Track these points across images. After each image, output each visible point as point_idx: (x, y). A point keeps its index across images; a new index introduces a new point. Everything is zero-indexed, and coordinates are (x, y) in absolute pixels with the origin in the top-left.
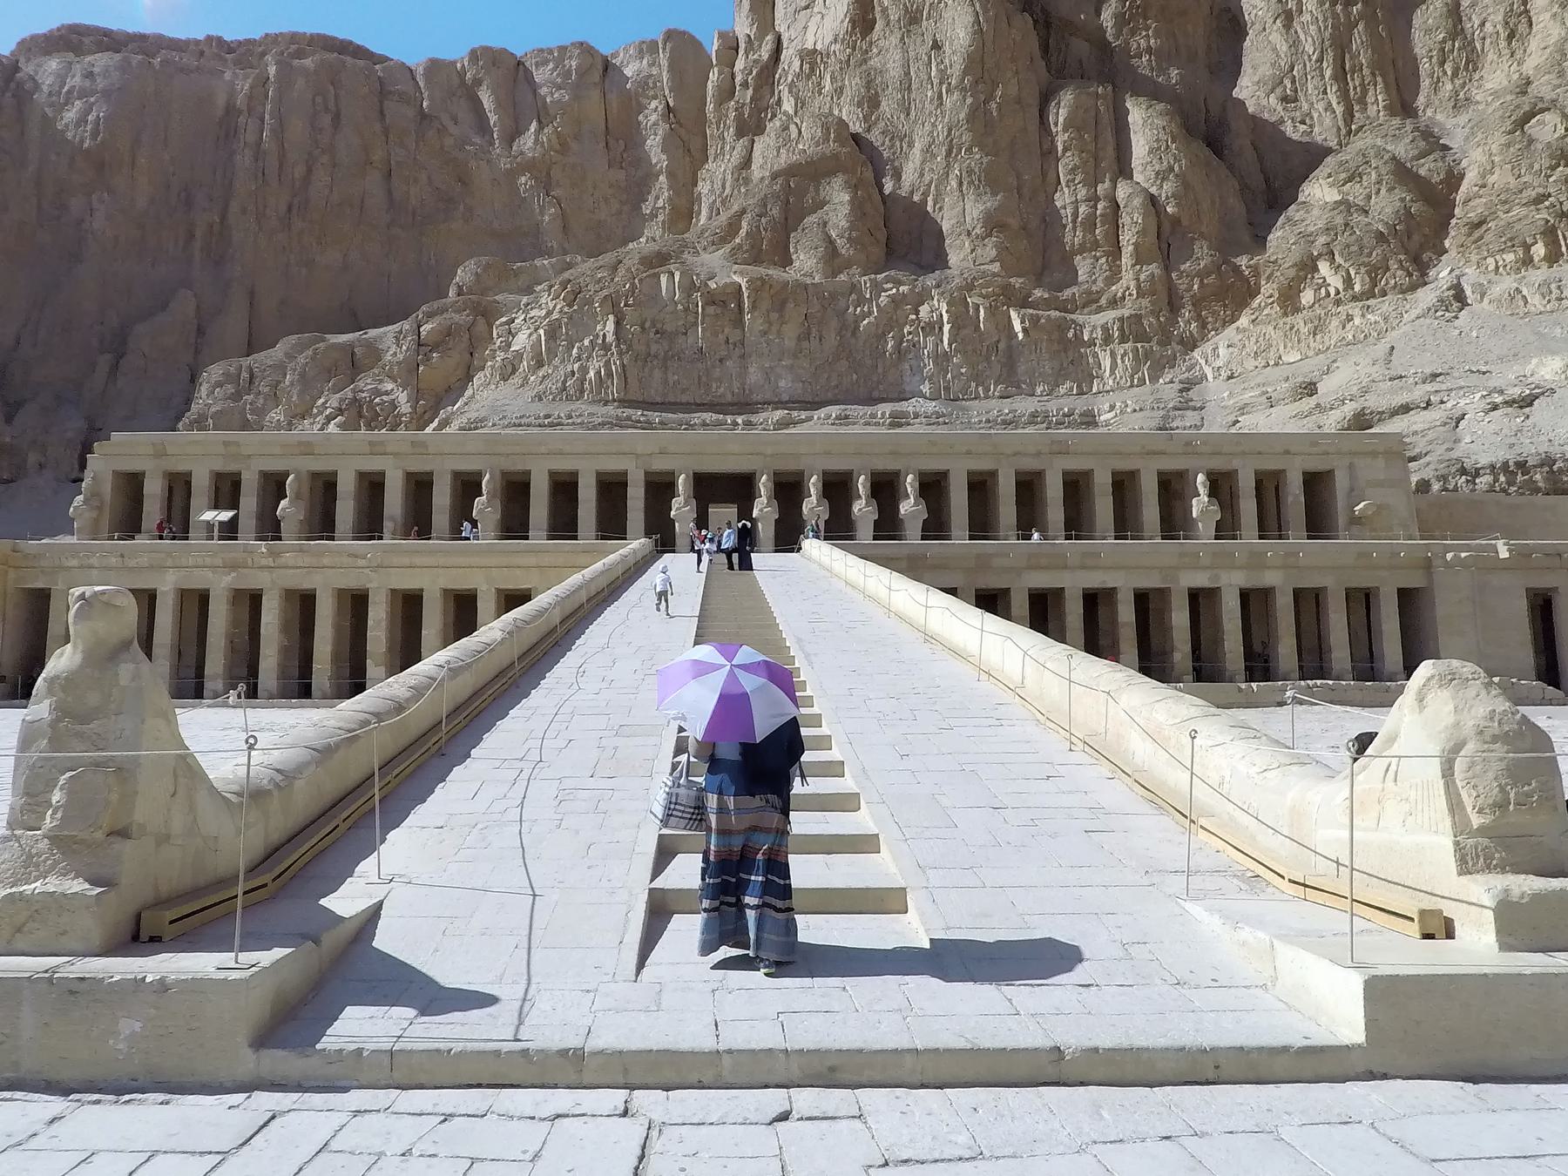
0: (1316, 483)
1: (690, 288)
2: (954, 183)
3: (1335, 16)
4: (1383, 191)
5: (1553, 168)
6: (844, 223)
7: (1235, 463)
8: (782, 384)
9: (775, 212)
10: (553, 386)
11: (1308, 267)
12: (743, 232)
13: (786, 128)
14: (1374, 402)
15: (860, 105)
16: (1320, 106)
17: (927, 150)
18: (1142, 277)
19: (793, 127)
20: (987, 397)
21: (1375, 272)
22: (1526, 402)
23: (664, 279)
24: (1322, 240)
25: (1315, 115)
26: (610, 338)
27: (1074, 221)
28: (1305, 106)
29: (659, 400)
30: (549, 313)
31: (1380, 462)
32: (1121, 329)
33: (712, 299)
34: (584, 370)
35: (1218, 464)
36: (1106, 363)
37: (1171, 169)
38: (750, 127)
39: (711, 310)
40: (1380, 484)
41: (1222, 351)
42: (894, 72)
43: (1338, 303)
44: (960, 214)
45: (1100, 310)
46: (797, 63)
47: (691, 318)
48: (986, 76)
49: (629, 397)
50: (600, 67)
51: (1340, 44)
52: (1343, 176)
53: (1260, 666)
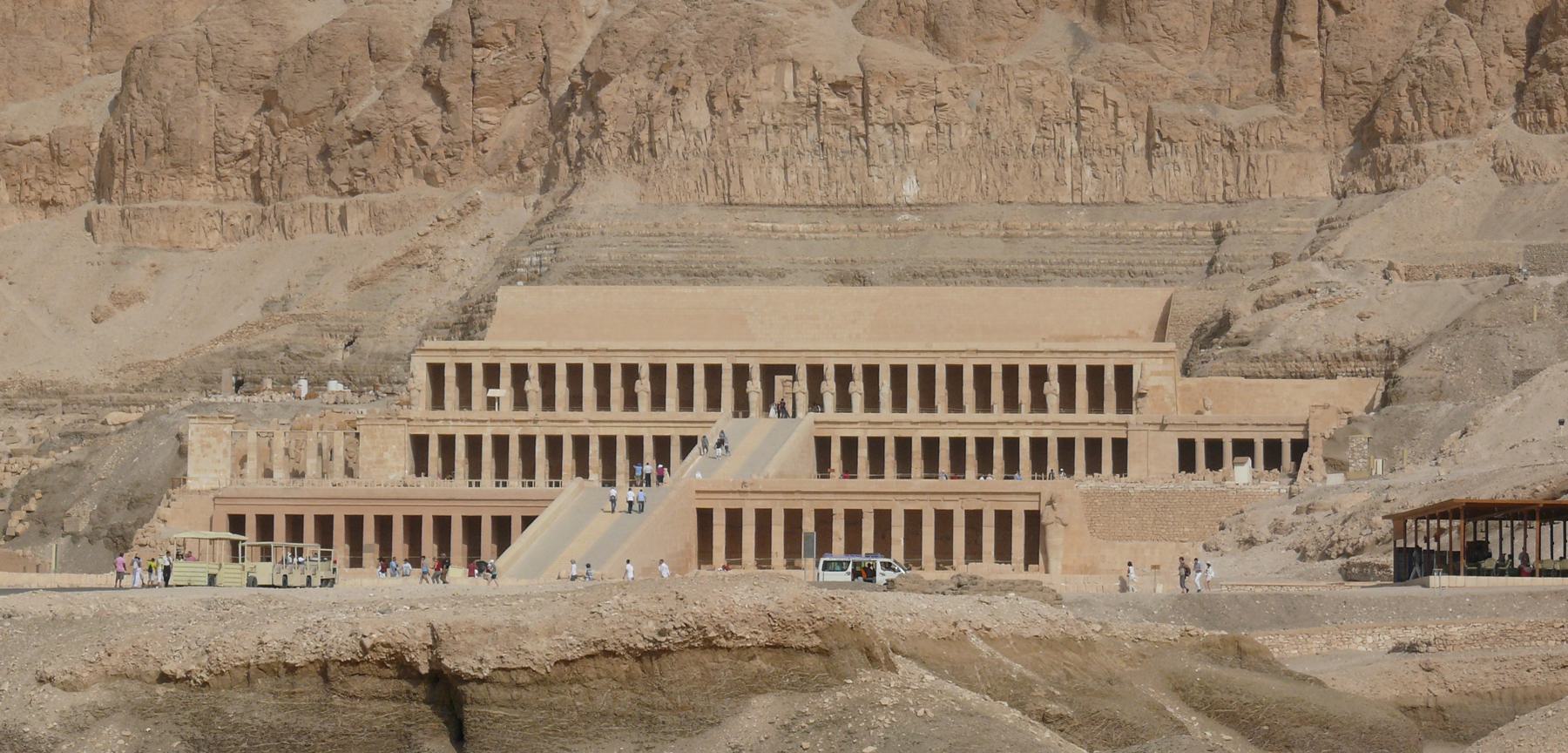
0: (1124, 373)
8: (906, 187)
14: (1281, 287)
22: (1327, 304)
39: (833, 101)
40: (1158, 374)
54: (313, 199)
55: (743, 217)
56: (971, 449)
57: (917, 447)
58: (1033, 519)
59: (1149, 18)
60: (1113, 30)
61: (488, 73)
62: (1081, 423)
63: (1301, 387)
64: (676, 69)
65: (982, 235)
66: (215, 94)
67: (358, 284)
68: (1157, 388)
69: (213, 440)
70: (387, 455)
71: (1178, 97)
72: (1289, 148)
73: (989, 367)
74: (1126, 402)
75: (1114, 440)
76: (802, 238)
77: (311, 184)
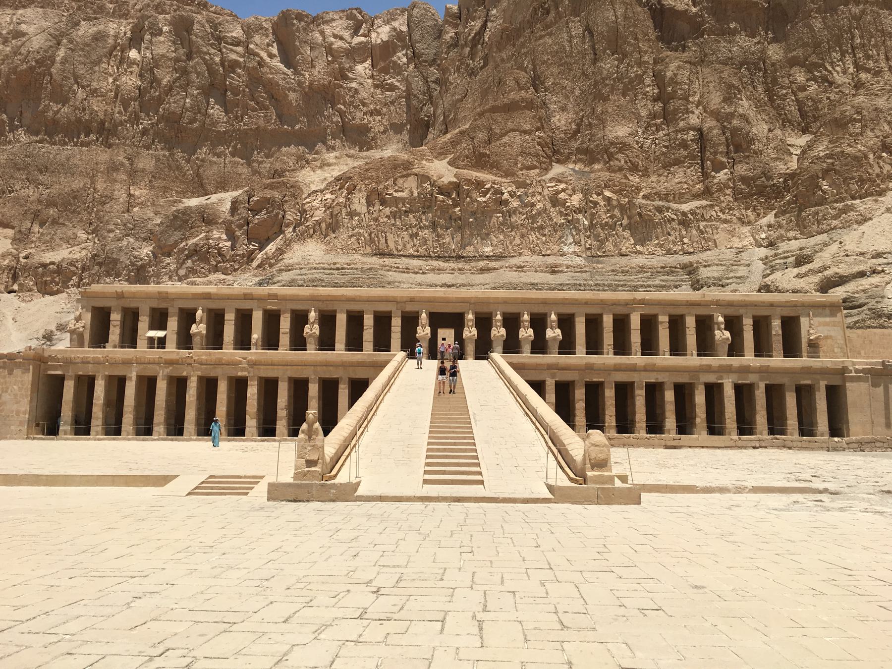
0: (790, 325)
4: (868, 131)
7: (742, 311)
9: (481, 136)
14: (843, 270)
18: (715, 181)
20: (612, 256)
28: (830, 68)
31: (827, 311)
35: (730, 312)
39: (441, 197)
40: (826, 324)
43: (836, 201)
53: (745, 427)
55: (388, 261)
56: (669, 396)
59: (620, 156)
60: (597, 166)
61: (256, 221)
65: (536, 271)
66: (132, 240)
68: (826, 337)
71: (644, 197)
72: (725, 221)
73: (655, 316)
76: (424, 273)
77: (170, 278)
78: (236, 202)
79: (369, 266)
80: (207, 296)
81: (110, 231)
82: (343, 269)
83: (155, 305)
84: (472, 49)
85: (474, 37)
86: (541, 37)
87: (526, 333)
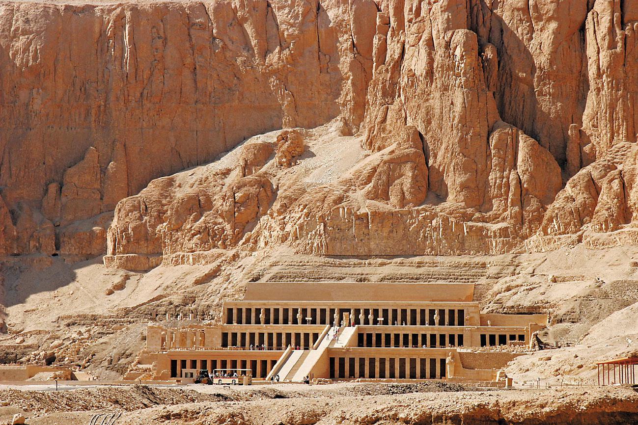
0: (461, 312)
1: (350, 213)
2: (452, 168)
3: (611, 95)
4: (581, 193)
5: (614, 199)
6: (408, 185)
10: (301, 248)
11: (551, 220)
12: (371, 185)
13: (401, 110)
14: (514, 284)
15: (424, 122)
16: (604, 132)
17: (446, 149)
19: (403, 111)
21: (567, 225)
22: (531, 289)
23: (341, 210)
24: (556, 211)
25: (602, 136)
26: (322, 232)
27: (495, 185)
29: (339, 254)
30: (300, 218)
32: (500, 233)
33: (358, 218)
34: (313, 243)
36: (494, 244)
37: (527, 170)
38: (390, 92)
39: (358, 222)
40: (473, 312)
41: (532, 242)
42: (437, 111)
43: (555, 235)
44: (453, 180)
45: (498, 222)
46: (406, 79)
47: (351, 225)
48: (467, 124)
49: (329, 254)
50: (315, 10)
51: (612, 107)
52: (572, 185)
54: (182, 254)
56: (410, 338)
57: (392, 337)
58: (443, 362)
62: (447, 330)
63: (520, 317)
64: (305, 210)
67: (198, 282)
69: (155, 335)
70: (214, 339)
74: (461, 323)
75: (459, 335)
78: (225, 196)
79: (318, 264)
80: (265, 304)
81: (131, 211)
82: (305, 265)
83: (247, 308)
84: (392, 74)
85: (394, 66)
86: (428, 100)
87: (370, 317)
